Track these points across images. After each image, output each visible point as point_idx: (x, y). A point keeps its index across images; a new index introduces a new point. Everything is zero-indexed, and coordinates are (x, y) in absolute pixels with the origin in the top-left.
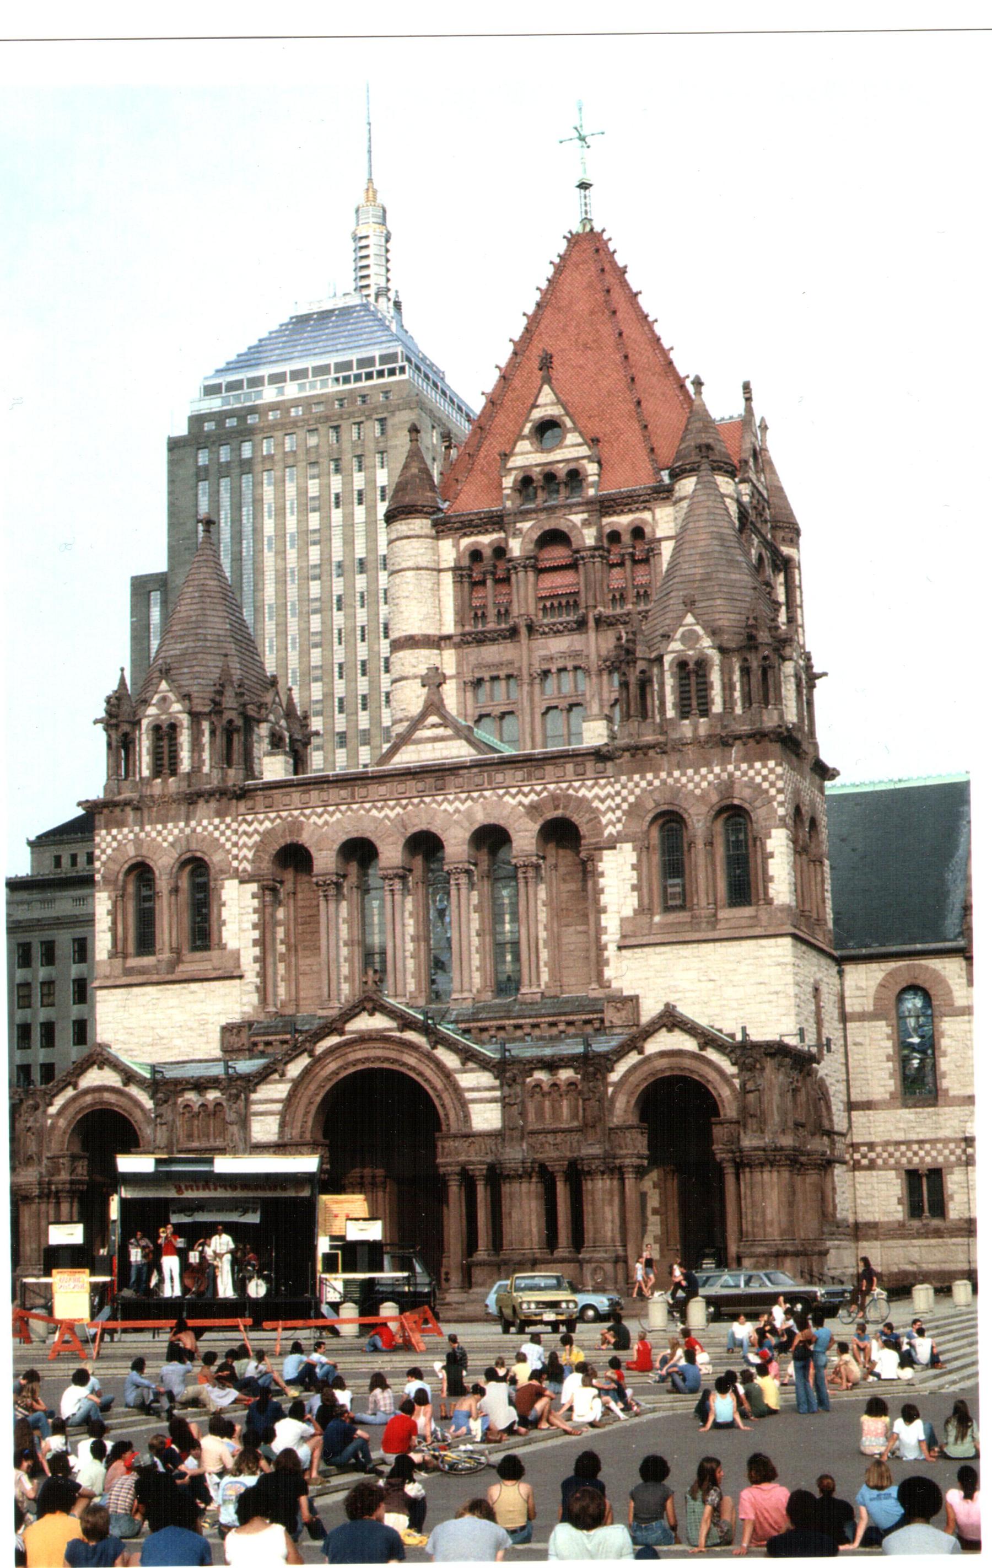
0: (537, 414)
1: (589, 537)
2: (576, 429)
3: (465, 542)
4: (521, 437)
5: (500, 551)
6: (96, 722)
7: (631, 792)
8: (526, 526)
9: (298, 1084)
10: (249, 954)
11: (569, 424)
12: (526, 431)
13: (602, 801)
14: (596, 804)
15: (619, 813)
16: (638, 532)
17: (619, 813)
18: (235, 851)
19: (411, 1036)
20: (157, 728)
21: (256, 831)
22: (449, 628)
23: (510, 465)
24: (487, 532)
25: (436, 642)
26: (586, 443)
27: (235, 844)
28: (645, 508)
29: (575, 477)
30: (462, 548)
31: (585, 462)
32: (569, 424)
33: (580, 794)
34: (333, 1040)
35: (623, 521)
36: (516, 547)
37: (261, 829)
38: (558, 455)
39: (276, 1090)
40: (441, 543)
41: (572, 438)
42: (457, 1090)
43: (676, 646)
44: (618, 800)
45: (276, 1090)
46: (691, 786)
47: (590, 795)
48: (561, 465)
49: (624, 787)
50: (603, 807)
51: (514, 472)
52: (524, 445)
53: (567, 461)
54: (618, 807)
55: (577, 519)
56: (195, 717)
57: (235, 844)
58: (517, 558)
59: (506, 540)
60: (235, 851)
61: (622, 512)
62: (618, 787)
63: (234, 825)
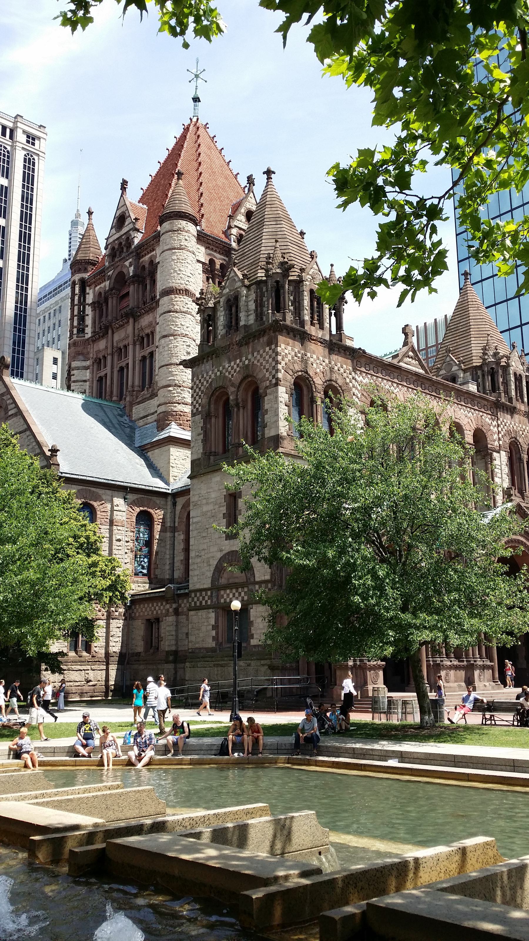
12: (243, 210)
18: (354, 389)
20: (312, 292)
24: (219, 253)
57: (354, 386)
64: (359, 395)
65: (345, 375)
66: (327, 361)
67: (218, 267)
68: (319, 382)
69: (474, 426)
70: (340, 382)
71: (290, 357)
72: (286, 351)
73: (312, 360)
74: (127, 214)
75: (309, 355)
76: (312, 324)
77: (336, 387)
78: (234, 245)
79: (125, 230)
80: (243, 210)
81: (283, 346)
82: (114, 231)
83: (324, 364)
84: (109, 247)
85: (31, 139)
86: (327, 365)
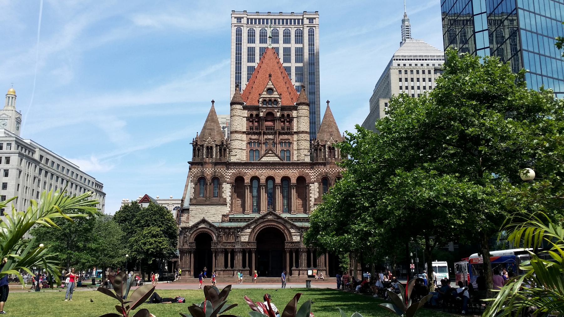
0: (268, 87)
1: (278, 115)
2: (276, 91)
4: (264, 91)
5: (257, 115)
6: (190, 143)
7: (318, 172)
8: (264, 110)
9: (253, 229)
10: (228, 200)
11: (275, 90)
12: (265, 90)
13: (311, 173)
14: (310, 174)
15: (315, 176)
16: (288, 115)
17: (315, 176)
18: (226, 176)
19: (279, 220)
20: (207, 147)
21: (231, 172)
22: (245, 130)
23: (261, 97)
25: (244, 133)
26: (278, 94)
27: (226, 175)
29: (276, 101)
32: (275, 90)
33: (306, 171)
34: (262, 220)
35: (286, 113)
36: (261, 114)
37: (232, 172)
38: (272, 96)
39: (249, 230)
40: (244, 111)
41: (276, 93)
42: (290, 233)
43: (328, 143)
44: (315, 173)
45: (249, 230)
46: (331, 172)
47: (309, 172)
49: (316, 171)
50: (311, 175)
53: (274, 98)
54: (315, 175)
55: (275, 110)
56: (217, 146)
57: (226, 175)
58: (262, 117)
59: (259, 113)
60: (226, 176)
62: (315, 171)
63: (226, 171)
64: (229, 178)
65: (222, 172)
66: (213, 169)
67: (254, 116)
68: (209, 178)
69: (298, 175)
70: (219, 175)
71: (196, 172)
72: (194, 171)
73: (206, 171)
75: (205, 169)
76: (207, 157)
77: (218, 177)
81: (193, 169)
83: (212, 171)
85: (311, 20)
86: (213, 171)
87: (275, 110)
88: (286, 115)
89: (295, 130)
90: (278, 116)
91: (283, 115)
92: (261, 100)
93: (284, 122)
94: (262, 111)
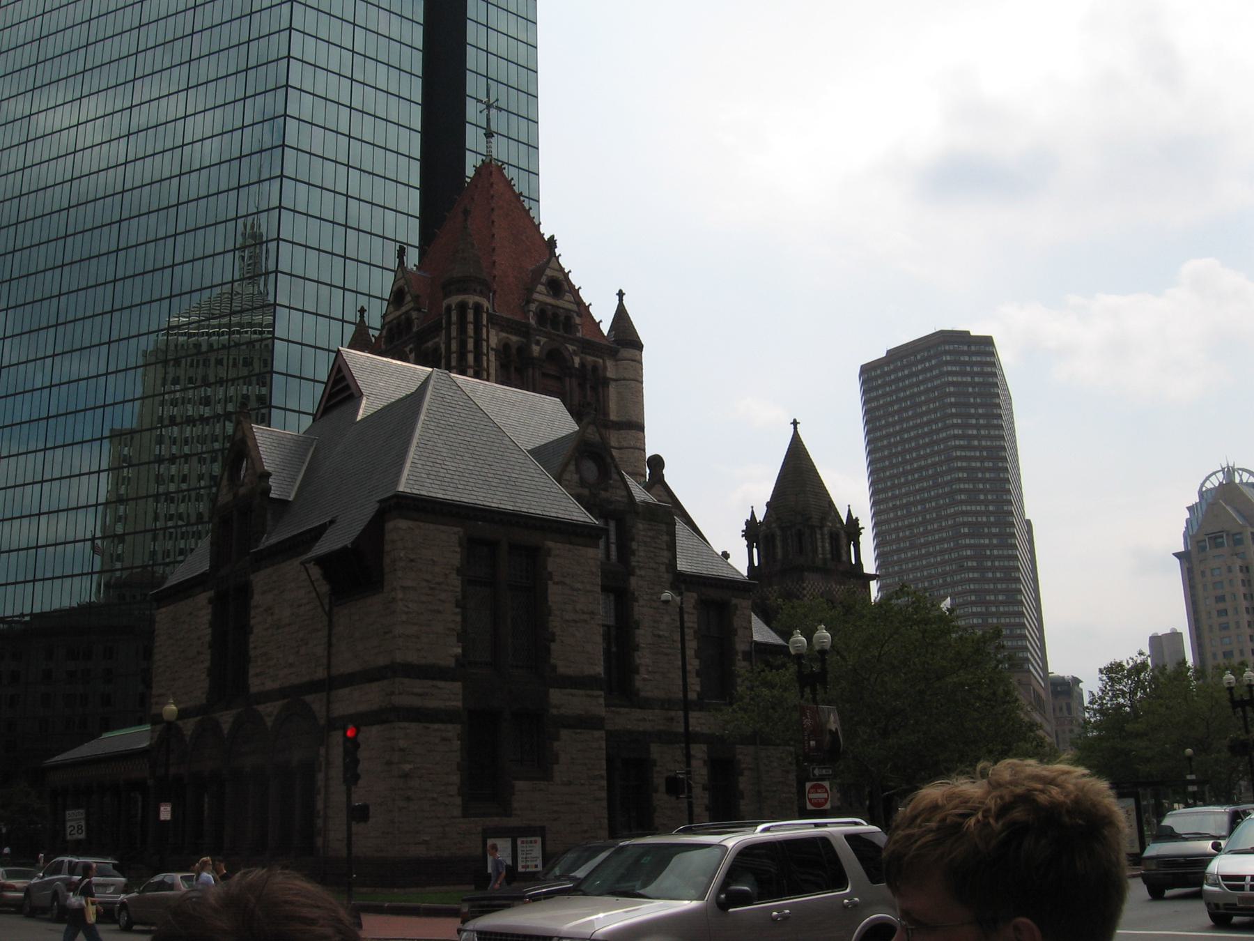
1: (577, 360)
3: (504, 335)
5: (523, 350)
8: (543, 340)
12: (544, 279)
16: (595, 368)
24: (515, 334)
28: (600, 357)
30: (500, 337)
31: (575, 315)
32: (567, 288)
35: (590, 358)
36: (536, 349)
48: (562, 311)
51: (537, 303)
52: (540, 288)
55: (571, 348)
61: (589, 354)
67: (514, 351)
74: (406, 289)
78: (532, 322)
79: (404, 309)
80: (544, 279)
82: (391, 308)
84: (386, 327)
87: (568, 345)
88: (589, 367)
89: (613, 417)
90: (577, 365)
91: (583, 365)
92: (533, 307)
93: (582, 386)
94: (538, 343)
